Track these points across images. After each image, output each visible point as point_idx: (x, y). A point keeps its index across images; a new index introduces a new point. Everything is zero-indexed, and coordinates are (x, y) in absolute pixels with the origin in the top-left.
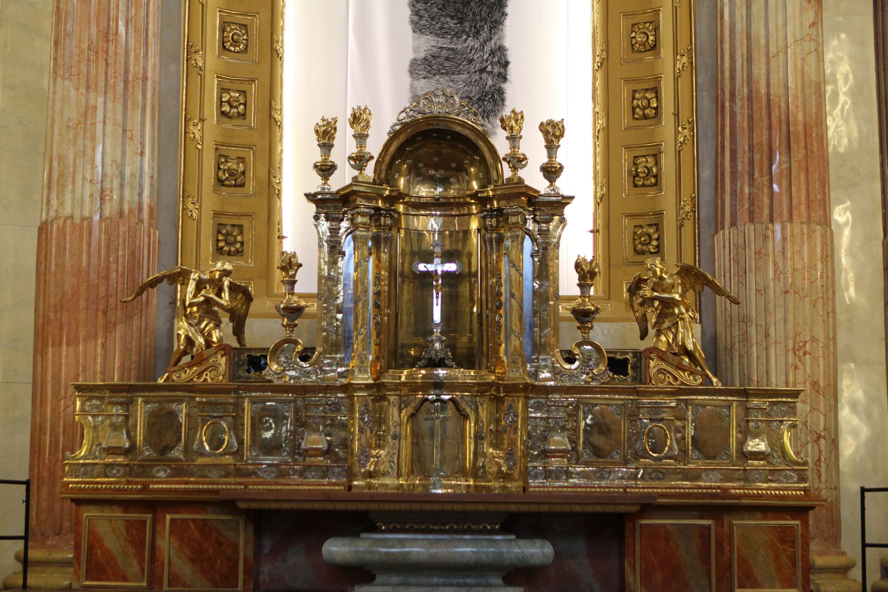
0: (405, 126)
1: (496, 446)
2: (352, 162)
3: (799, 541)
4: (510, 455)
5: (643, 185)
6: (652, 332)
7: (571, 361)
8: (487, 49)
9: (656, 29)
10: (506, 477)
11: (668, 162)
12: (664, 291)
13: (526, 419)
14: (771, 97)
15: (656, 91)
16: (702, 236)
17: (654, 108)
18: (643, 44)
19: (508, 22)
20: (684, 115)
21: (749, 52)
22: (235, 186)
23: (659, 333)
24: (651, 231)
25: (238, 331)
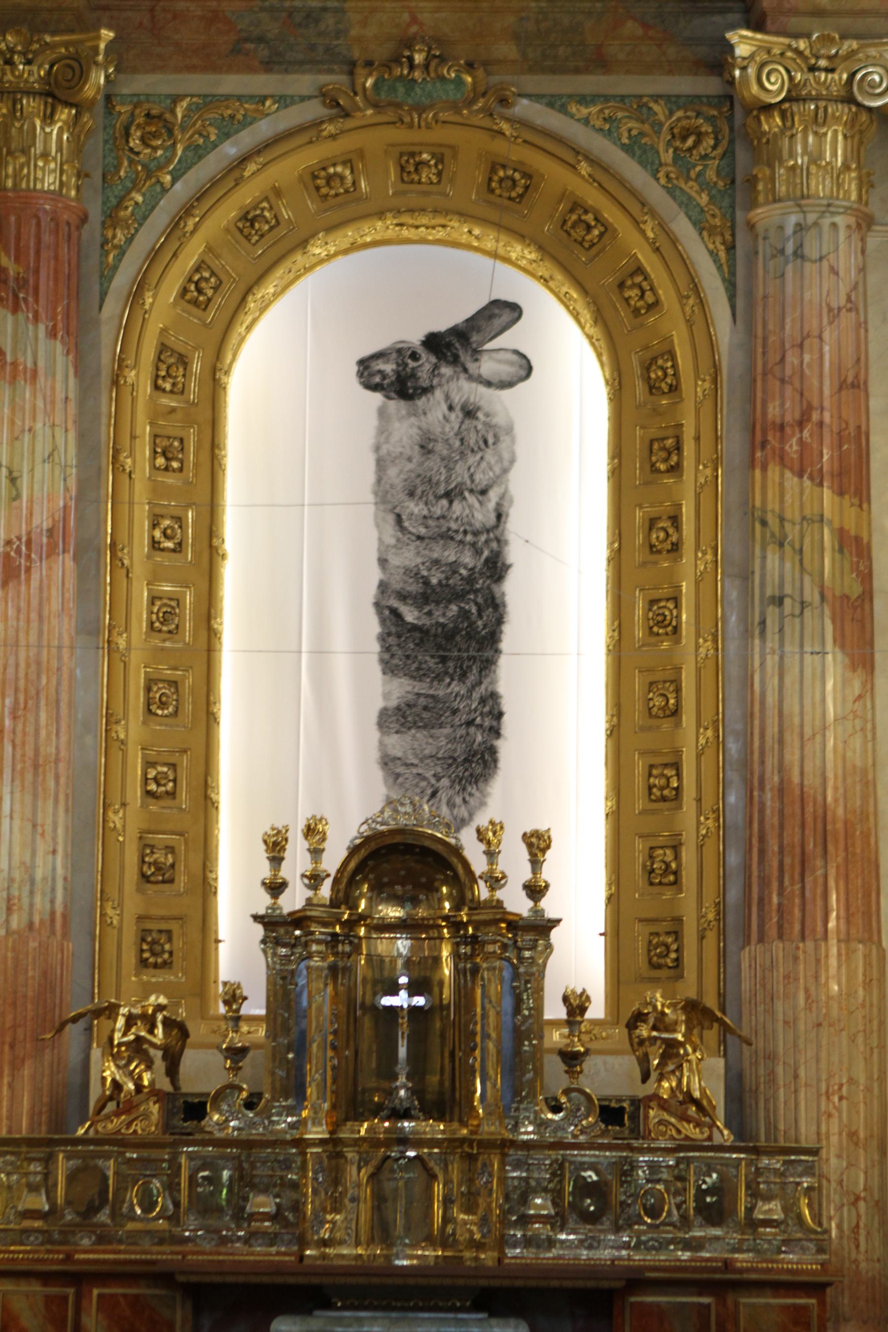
0: (367, 840)
1: (469, 1210)
2: (306, 881)
3: (815, 1322)
4: (484, 1221)
5: (660, 883)
6: (654, 1076)
7: (556, 1109)
8: (476, 695)
9: (678, 690)
10: (479, 1246)
11: (688, 855)
12: (667, 1030)
13: (503, 1180)
14: (805, 789)
15: (677, 766)
16: (728, 949)
17: (675, 789)
18: (662, 709)
19: (503, 662)
20: (708, 802)
21: (781, 732)
22: (163, 882)
23: (661, 1077)
24: (670, 940)
25: (172, 1071)
